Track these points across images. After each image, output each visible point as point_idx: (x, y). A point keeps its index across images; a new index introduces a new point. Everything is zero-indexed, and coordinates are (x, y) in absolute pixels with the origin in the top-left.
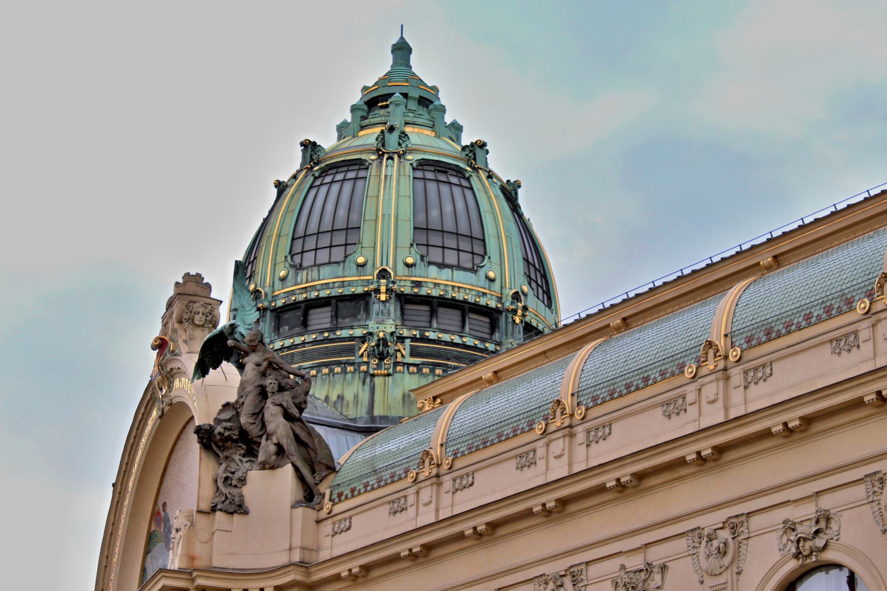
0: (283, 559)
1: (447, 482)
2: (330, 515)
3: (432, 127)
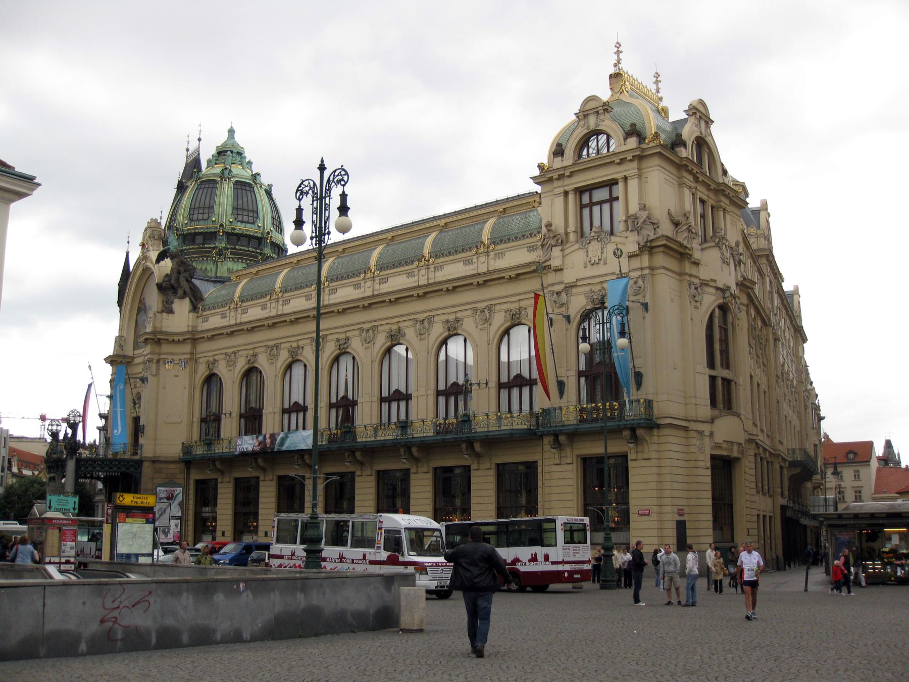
0: (185, 329)
1: (239, 310)
2: (201, 315)
3: (242, 165)
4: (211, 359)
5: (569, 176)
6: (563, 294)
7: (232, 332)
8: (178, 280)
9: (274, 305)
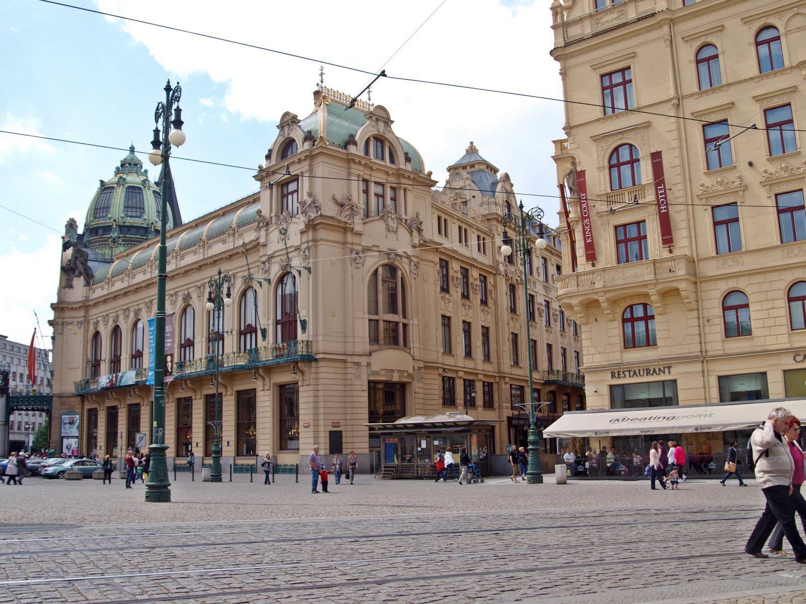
0: (80, 299)
6: (267, 263)
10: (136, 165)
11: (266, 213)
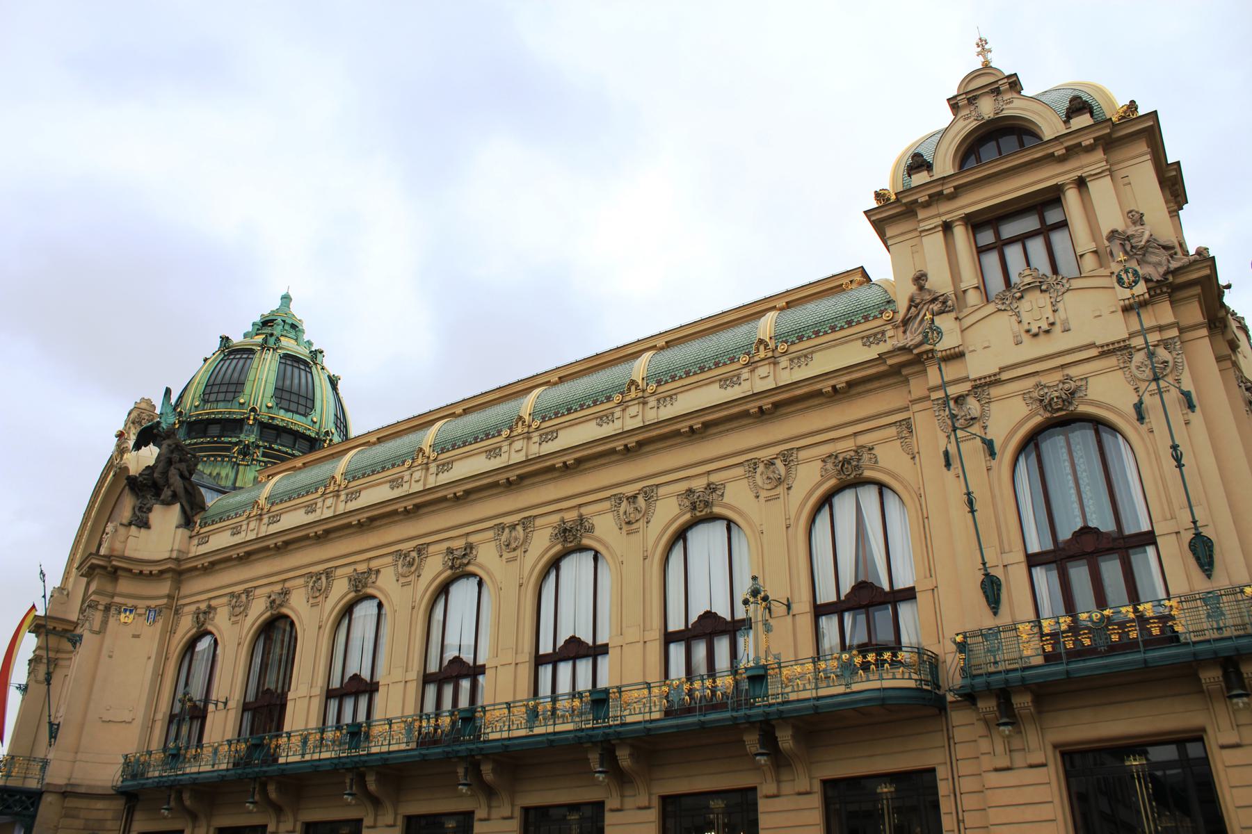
0: (167, 555)
2: (198, 534)
4: (203, 606)
5: (952, 197)
7: (249, 554)
8: (165, 473)
9: (329, 502)
10: (293, 326)
11: (940, 281)
